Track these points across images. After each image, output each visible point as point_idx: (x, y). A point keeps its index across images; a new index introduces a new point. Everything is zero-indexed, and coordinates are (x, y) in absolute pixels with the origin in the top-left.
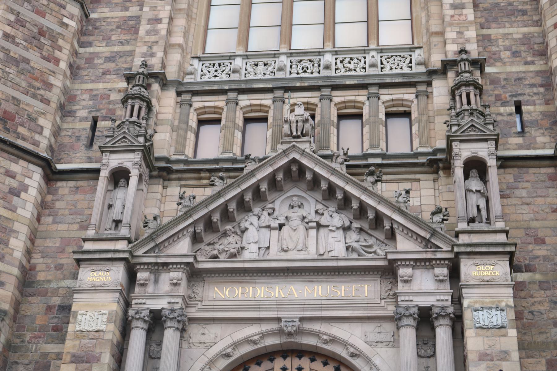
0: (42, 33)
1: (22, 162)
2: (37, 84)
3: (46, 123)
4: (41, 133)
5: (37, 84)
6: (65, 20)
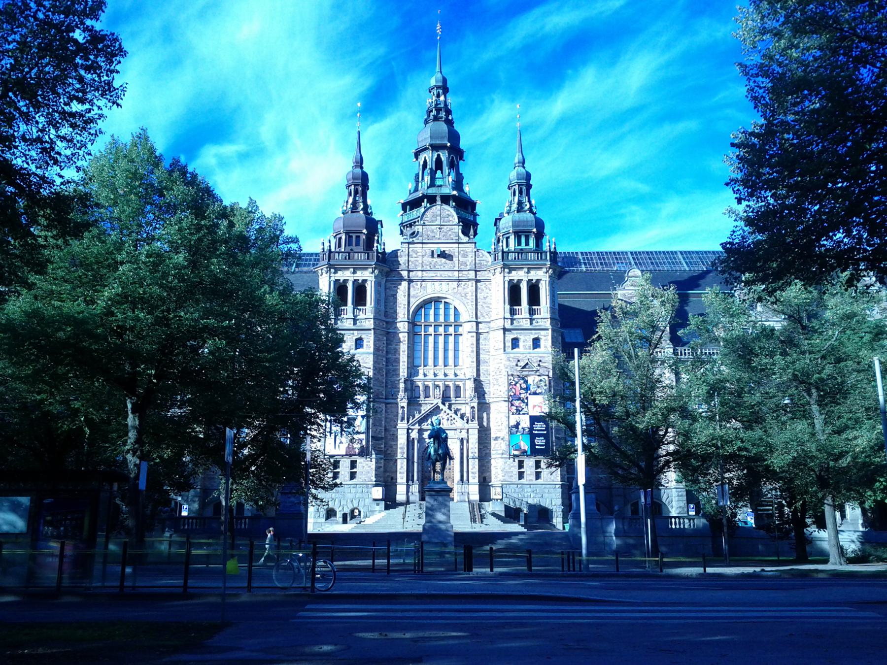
3: (384, 393)
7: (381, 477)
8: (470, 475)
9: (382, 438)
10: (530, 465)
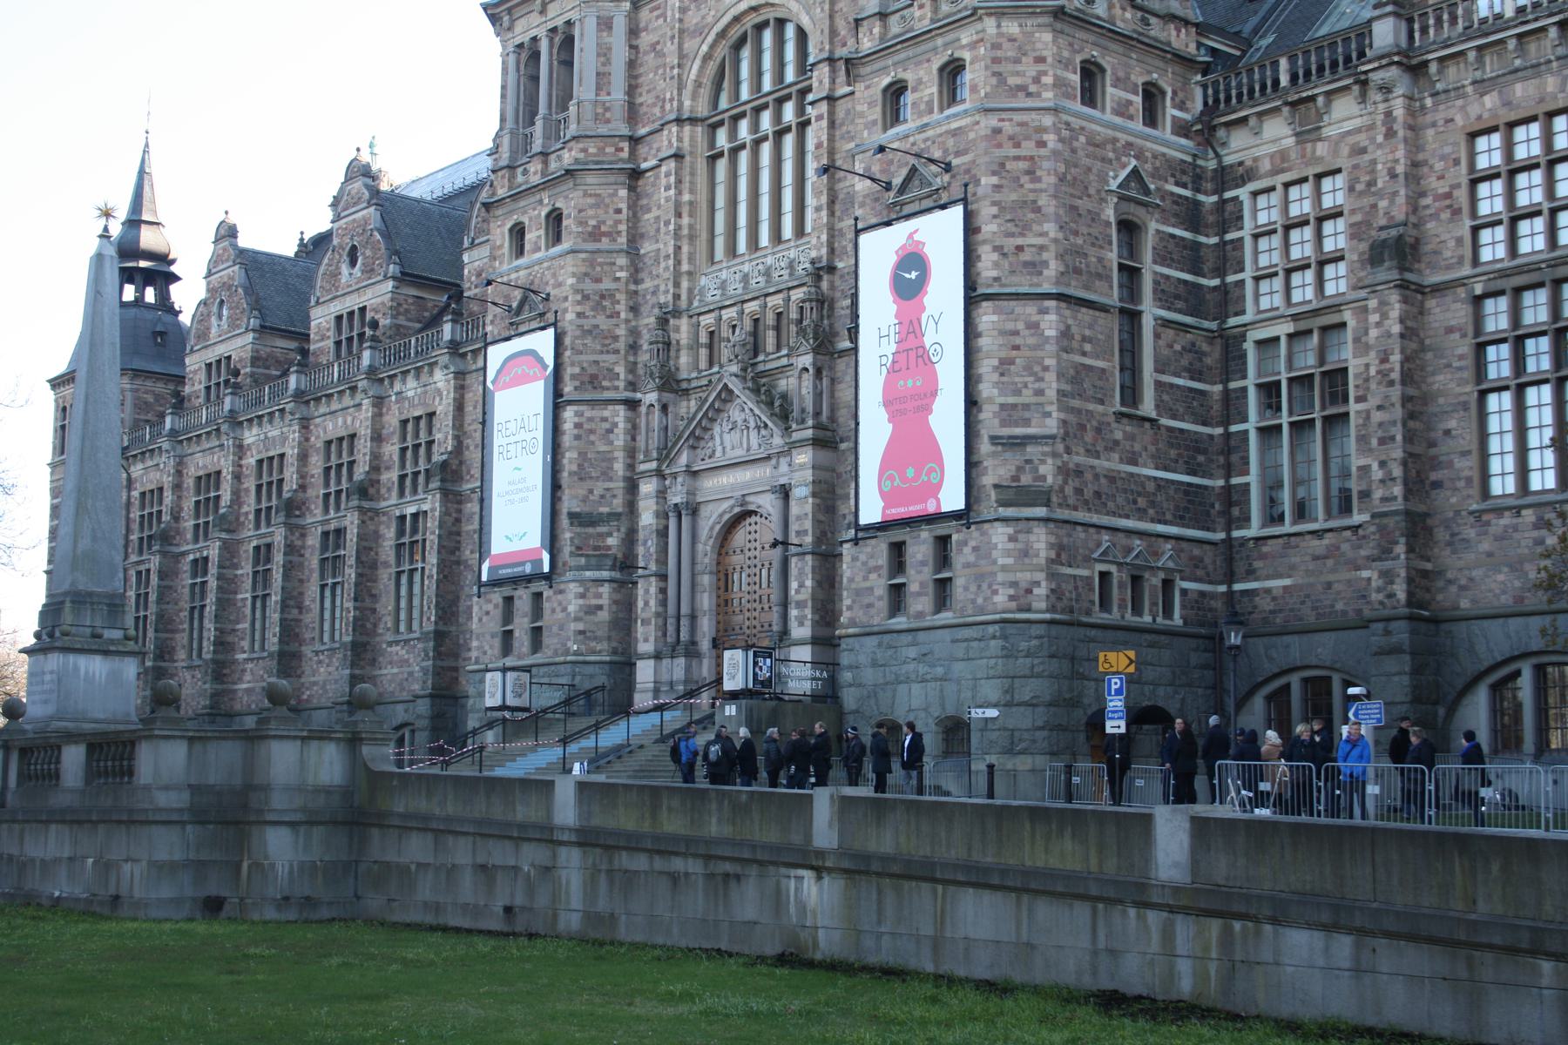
0: (603, 297)
1: (610, 407)
2: (607, 342)
3: (620, 370)
4: (618, 379)
5: (607, 342)
6: (618, 274)
7: (595, 638)
8: (793, 613)
9: (614, 516)
10: (919, 557)
